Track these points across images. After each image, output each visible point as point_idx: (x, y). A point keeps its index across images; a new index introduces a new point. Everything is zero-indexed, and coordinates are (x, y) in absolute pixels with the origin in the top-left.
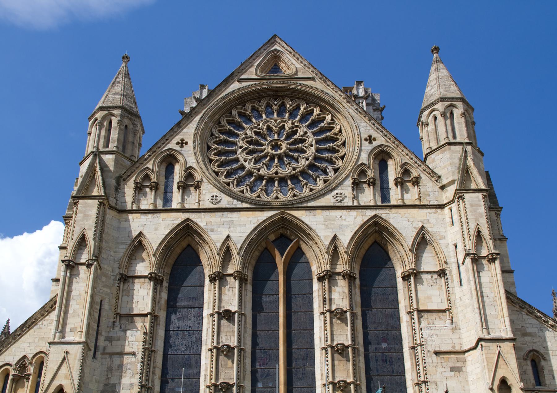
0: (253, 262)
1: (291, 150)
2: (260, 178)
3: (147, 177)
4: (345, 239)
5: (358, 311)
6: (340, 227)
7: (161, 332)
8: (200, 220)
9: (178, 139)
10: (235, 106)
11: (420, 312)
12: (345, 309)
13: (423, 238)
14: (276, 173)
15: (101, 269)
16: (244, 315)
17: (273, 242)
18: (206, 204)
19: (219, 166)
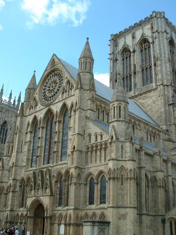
0: (46, 122)
1: (55, 87)
2: (49, 97)
3: (31, 105)
4: (58, 111)
5: (61, 130)
6: (58, 108)
7: (32, 145)
8: (37, 114)
9: (36, 93)
10: (47, 78)
11: (70, 128)
12: (57, 131)
13: (73, 105)
14: (52, 95)
15: (21, 132)
16: (43, 137)
17: (50, 115)
18: (39, 110)
19: (43, 97)
